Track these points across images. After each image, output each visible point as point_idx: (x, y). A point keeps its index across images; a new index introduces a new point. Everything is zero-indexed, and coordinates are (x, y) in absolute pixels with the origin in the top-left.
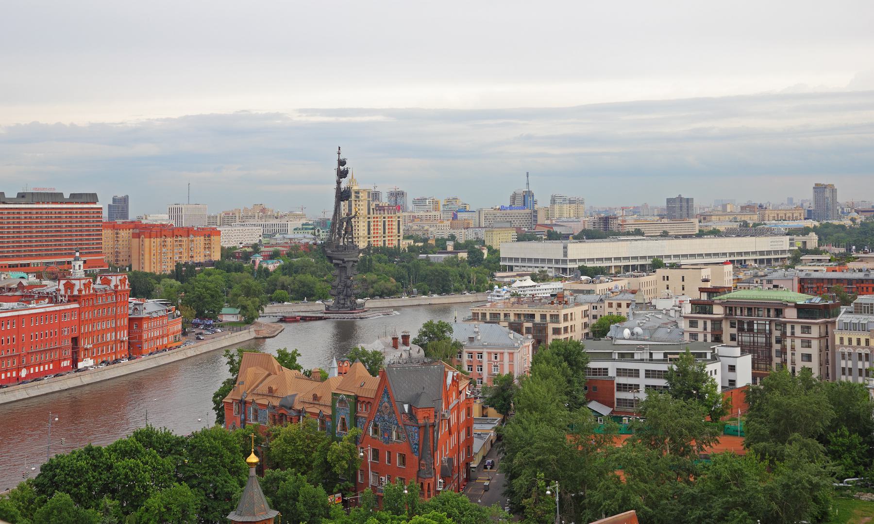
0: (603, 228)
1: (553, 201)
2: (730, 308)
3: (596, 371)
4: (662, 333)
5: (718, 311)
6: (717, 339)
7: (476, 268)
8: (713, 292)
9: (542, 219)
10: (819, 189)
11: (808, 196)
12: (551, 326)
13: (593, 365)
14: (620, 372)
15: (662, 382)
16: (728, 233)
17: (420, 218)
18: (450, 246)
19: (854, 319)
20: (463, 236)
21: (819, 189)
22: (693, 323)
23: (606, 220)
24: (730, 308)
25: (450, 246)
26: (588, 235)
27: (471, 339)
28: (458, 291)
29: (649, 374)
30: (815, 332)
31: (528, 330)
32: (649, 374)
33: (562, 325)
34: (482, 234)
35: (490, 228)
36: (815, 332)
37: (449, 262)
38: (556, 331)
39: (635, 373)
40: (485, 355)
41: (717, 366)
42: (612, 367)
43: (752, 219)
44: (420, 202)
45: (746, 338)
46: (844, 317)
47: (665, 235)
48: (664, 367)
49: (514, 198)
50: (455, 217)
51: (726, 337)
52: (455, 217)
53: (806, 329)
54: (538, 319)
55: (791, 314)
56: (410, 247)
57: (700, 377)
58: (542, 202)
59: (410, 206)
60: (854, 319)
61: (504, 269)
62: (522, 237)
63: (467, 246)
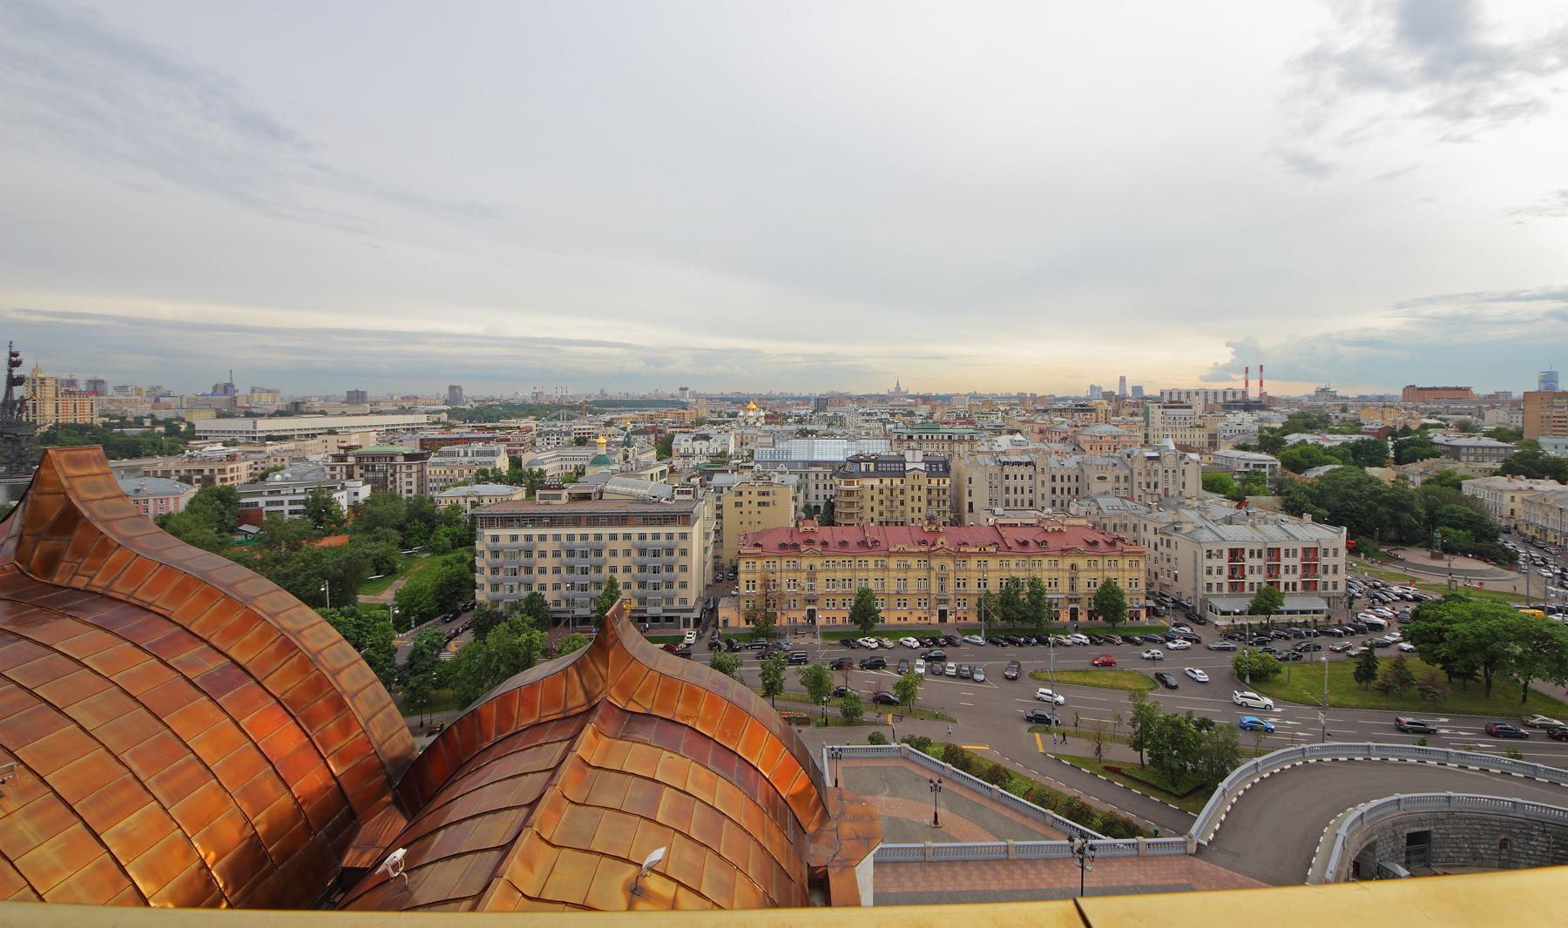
0: (295, 409)
1: (253, 391)
2: (359, 458)
3: (247, 504)
4: (310, 477)
5: (351, 460)
6: (350, 476)
7: (176, 437)
8: (347, 449)
9: (241, 402)
10: (452, 388)
11: (445, 392)
12: (218, 478)
13: (244, 500)
14: (268, 504)
15: (301, 507)
16: (394, 413)
17: (120, 401)
18: (147, 423)
19: (438, 460)
20: (161, 415)
21: (452, 388)
22: (333, 468)
23: (297, 405)
24: (359, 458)
25: (147, 423)
26: (280, 414)
27: (137, 491)
28: (148, 455)
29: (291, 503)
30: (415, 468)
31: (198, 481)
32: (291, 503)
33: (229, 475)
34: (182, 413)
35: (191, 409)
36: (415, 468)
37: (144, 435)
38: (224, 480)
39: (282, 503)
40: (151, 502)
41: (344, 493)
42: (261, 501)
43: (407, 405)
44: (122, 389)
45: (370, 475)
46: (432, 459)
47: (343, 414)
48: (303, 497)
49: (216, 388)
50: (157, 400)
51: (356, 475)
52: (157, 400)
53: (410, 467)
54: (207, 472)
55: (400, 460)
56: (104, 424)
57: (329, 501)
58: (242, 390)
59: (110, 391)
60: (438, 460)
61: (200, 438)
62: (221, 415)
63: (166, 422)
